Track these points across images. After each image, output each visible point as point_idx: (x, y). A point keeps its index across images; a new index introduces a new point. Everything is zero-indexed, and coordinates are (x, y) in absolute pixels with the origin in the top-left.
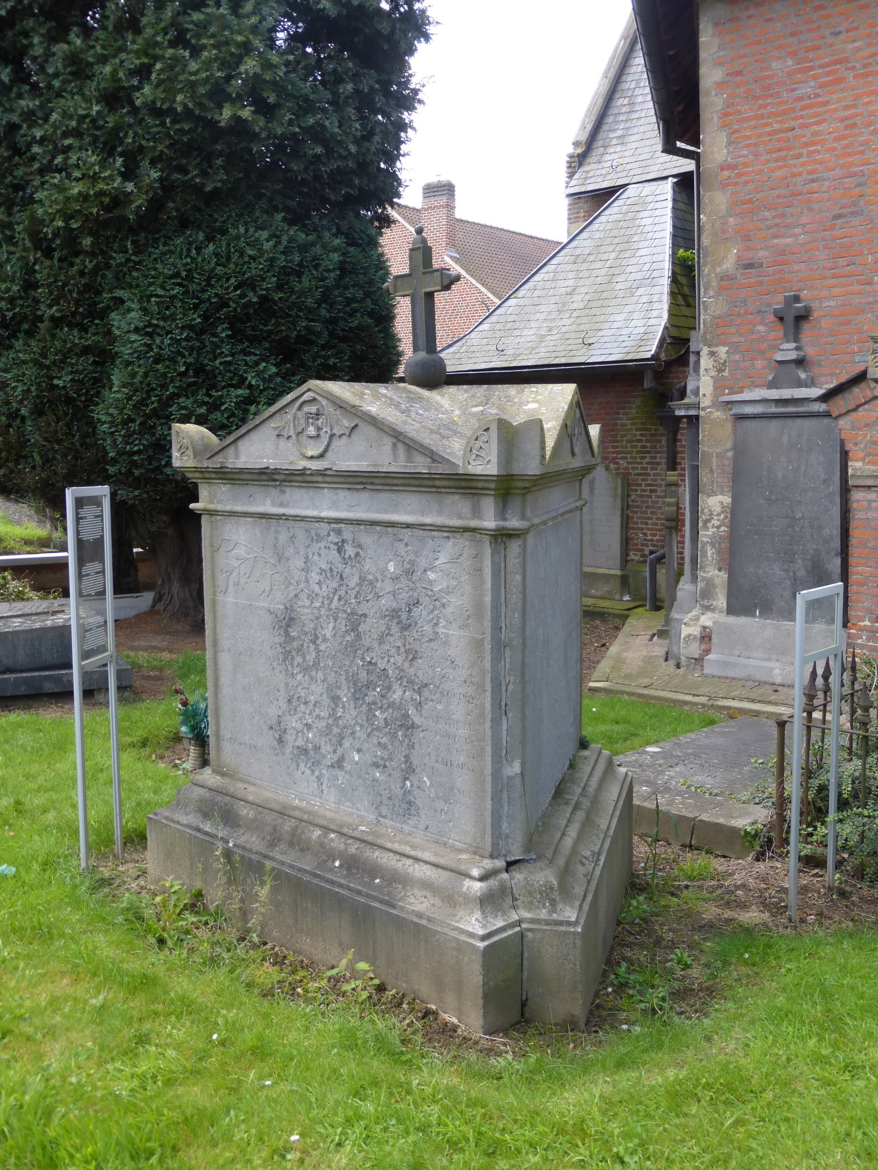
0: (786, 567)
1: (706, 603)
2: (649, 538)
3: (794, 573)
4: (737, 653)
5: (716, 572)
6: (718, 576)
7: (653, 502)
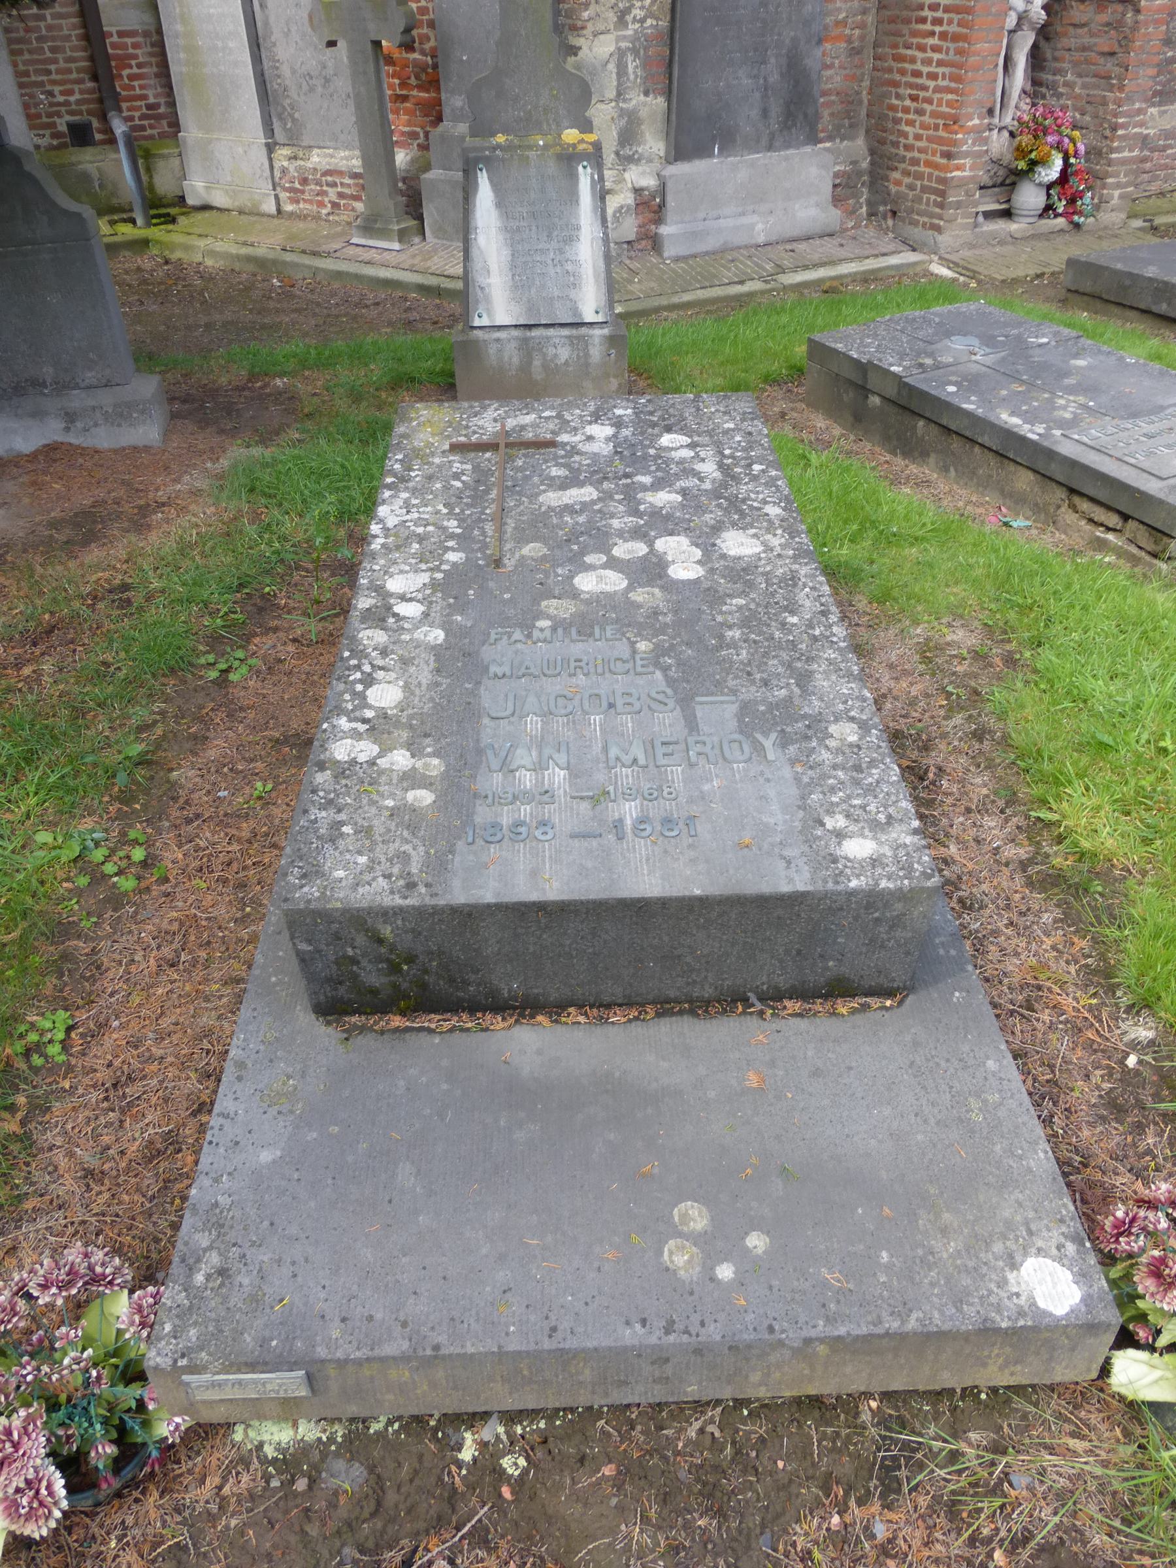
0: (755, 71)
1: (627, 151)
2: (61, 99)
3: (765, 79)
4: (701, 215)
5: (642, 97)
6: (645, 104)
7: (50, 28)
